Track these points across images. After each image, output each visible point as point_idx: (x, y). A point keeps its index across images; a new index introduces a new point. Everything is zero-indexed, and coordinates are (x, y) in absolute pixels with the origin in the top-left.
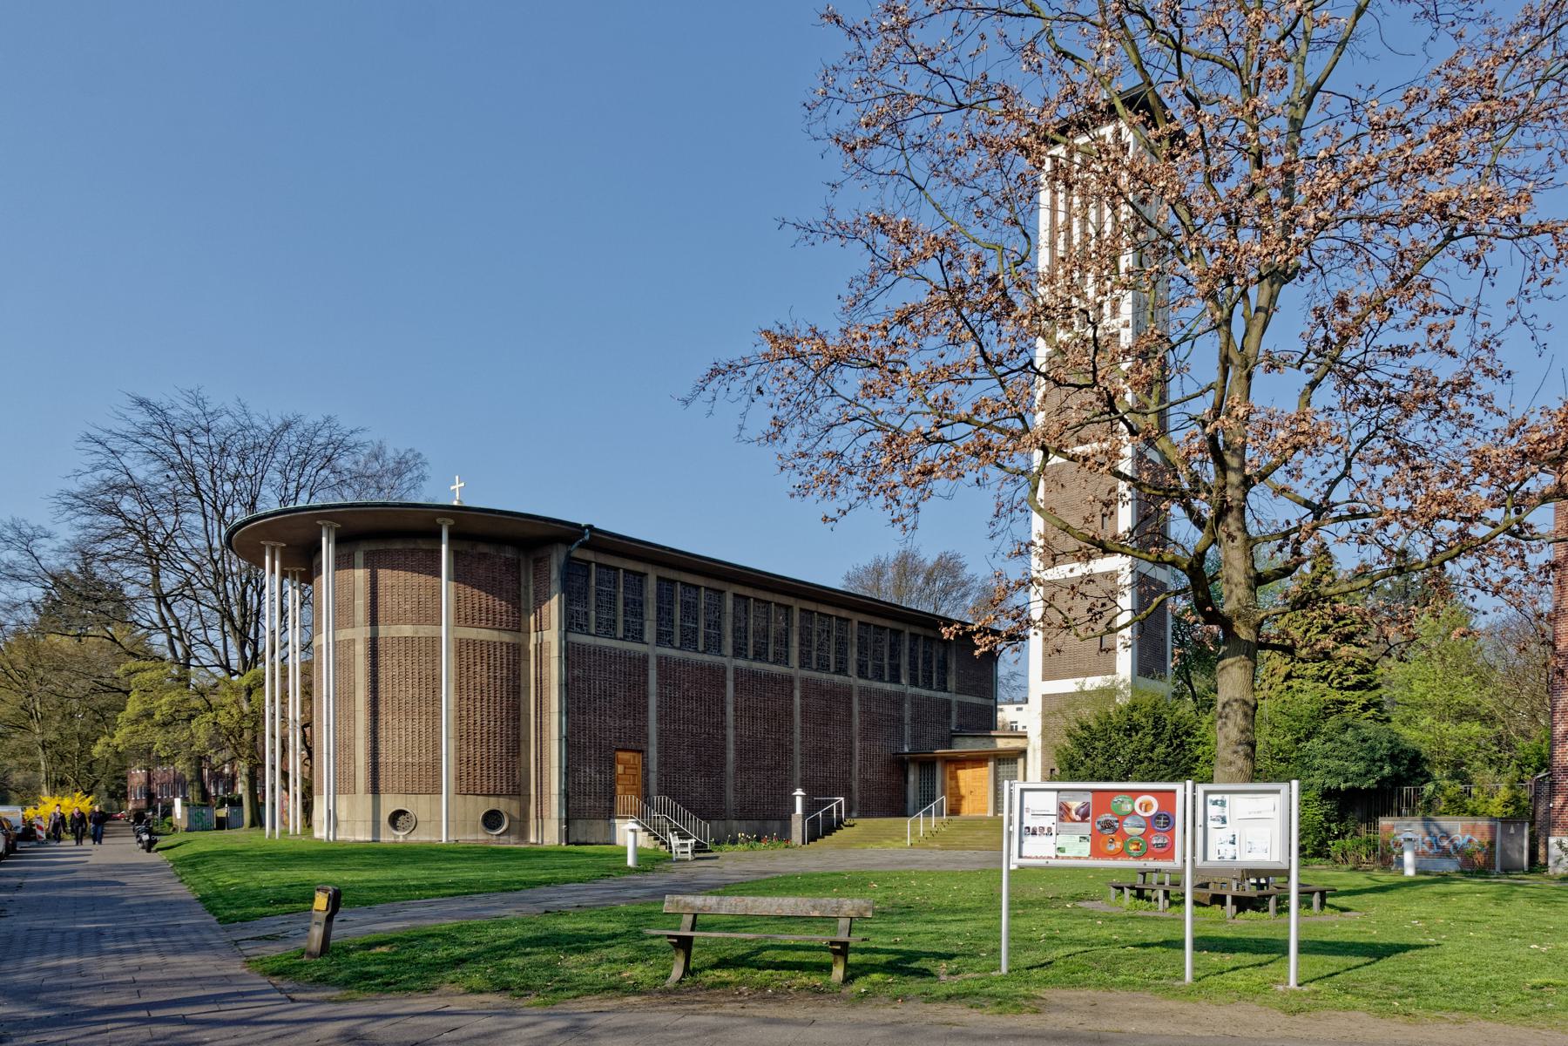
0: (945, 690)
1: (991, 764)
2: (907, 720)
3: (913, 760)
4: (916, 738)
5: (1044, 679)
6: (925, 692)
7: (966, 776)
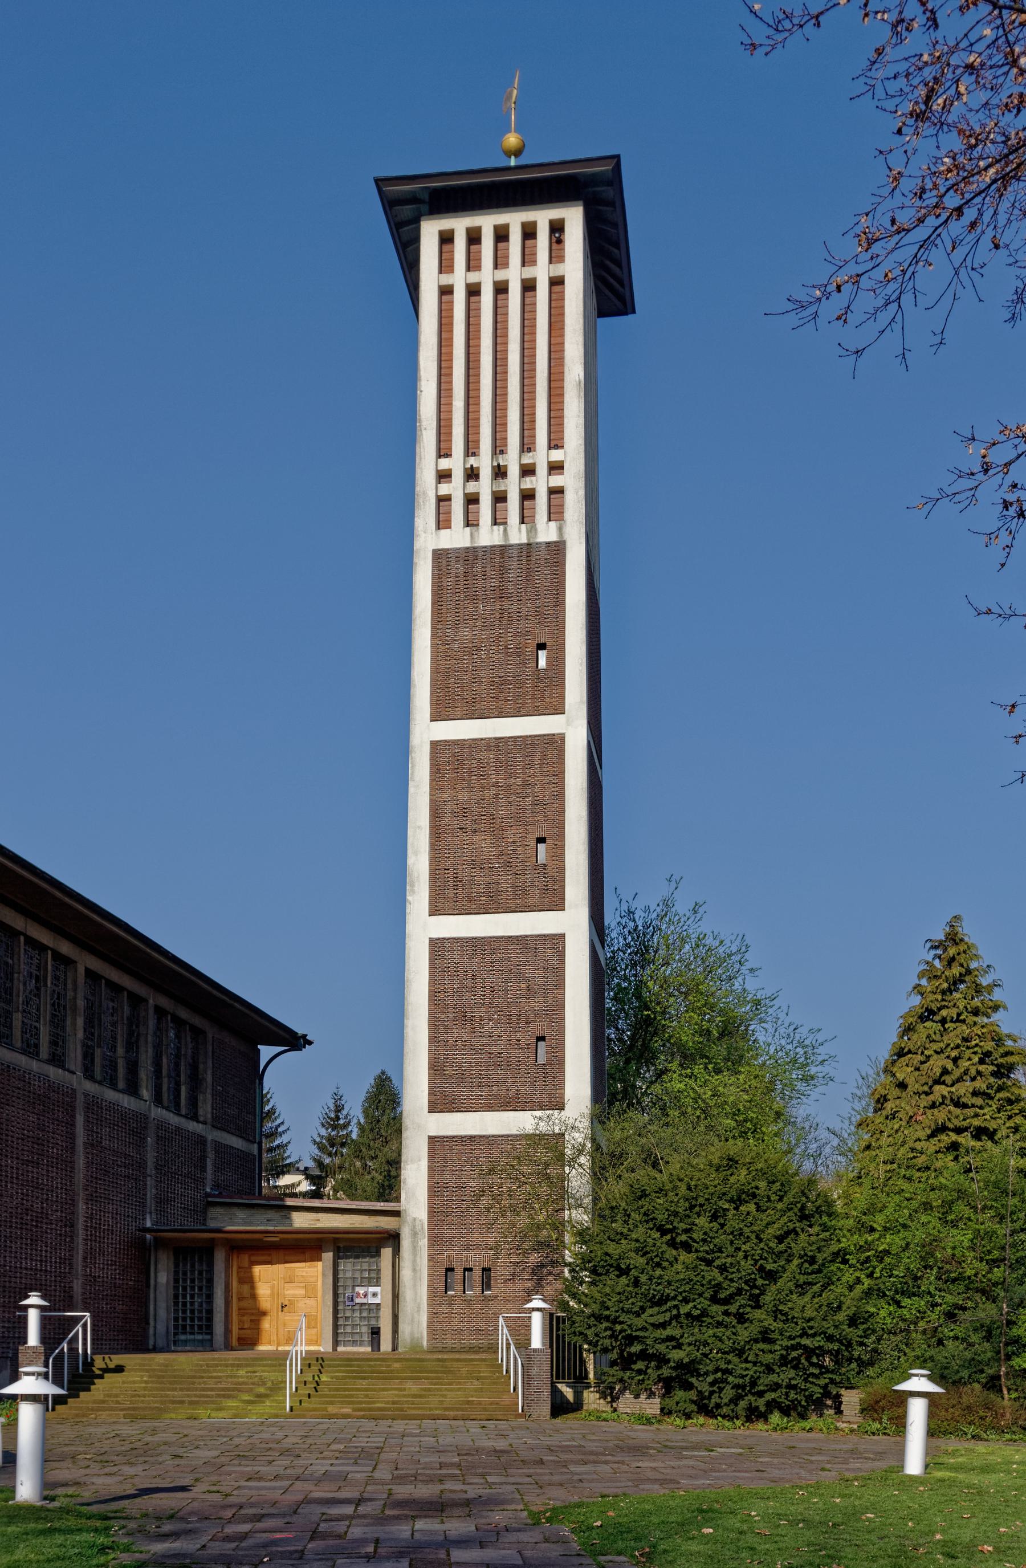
0: (195, 1118)
1: (328, 1256)
2: (150, 1169)
3: (160, 1243)
4: (162, 1202)
5: (432, 1109)
6: (174, 1119)
7: (270, 1280)
